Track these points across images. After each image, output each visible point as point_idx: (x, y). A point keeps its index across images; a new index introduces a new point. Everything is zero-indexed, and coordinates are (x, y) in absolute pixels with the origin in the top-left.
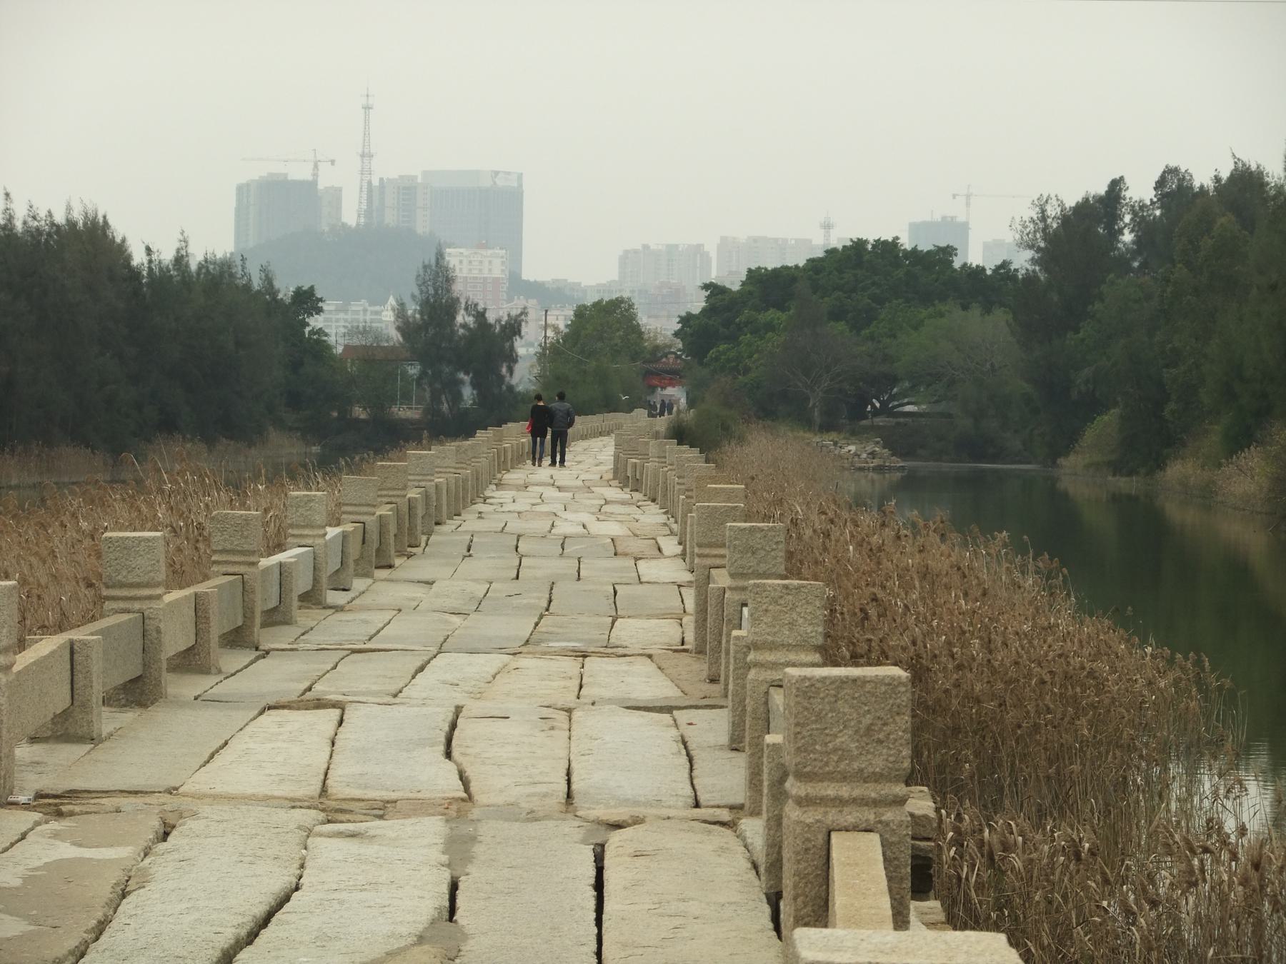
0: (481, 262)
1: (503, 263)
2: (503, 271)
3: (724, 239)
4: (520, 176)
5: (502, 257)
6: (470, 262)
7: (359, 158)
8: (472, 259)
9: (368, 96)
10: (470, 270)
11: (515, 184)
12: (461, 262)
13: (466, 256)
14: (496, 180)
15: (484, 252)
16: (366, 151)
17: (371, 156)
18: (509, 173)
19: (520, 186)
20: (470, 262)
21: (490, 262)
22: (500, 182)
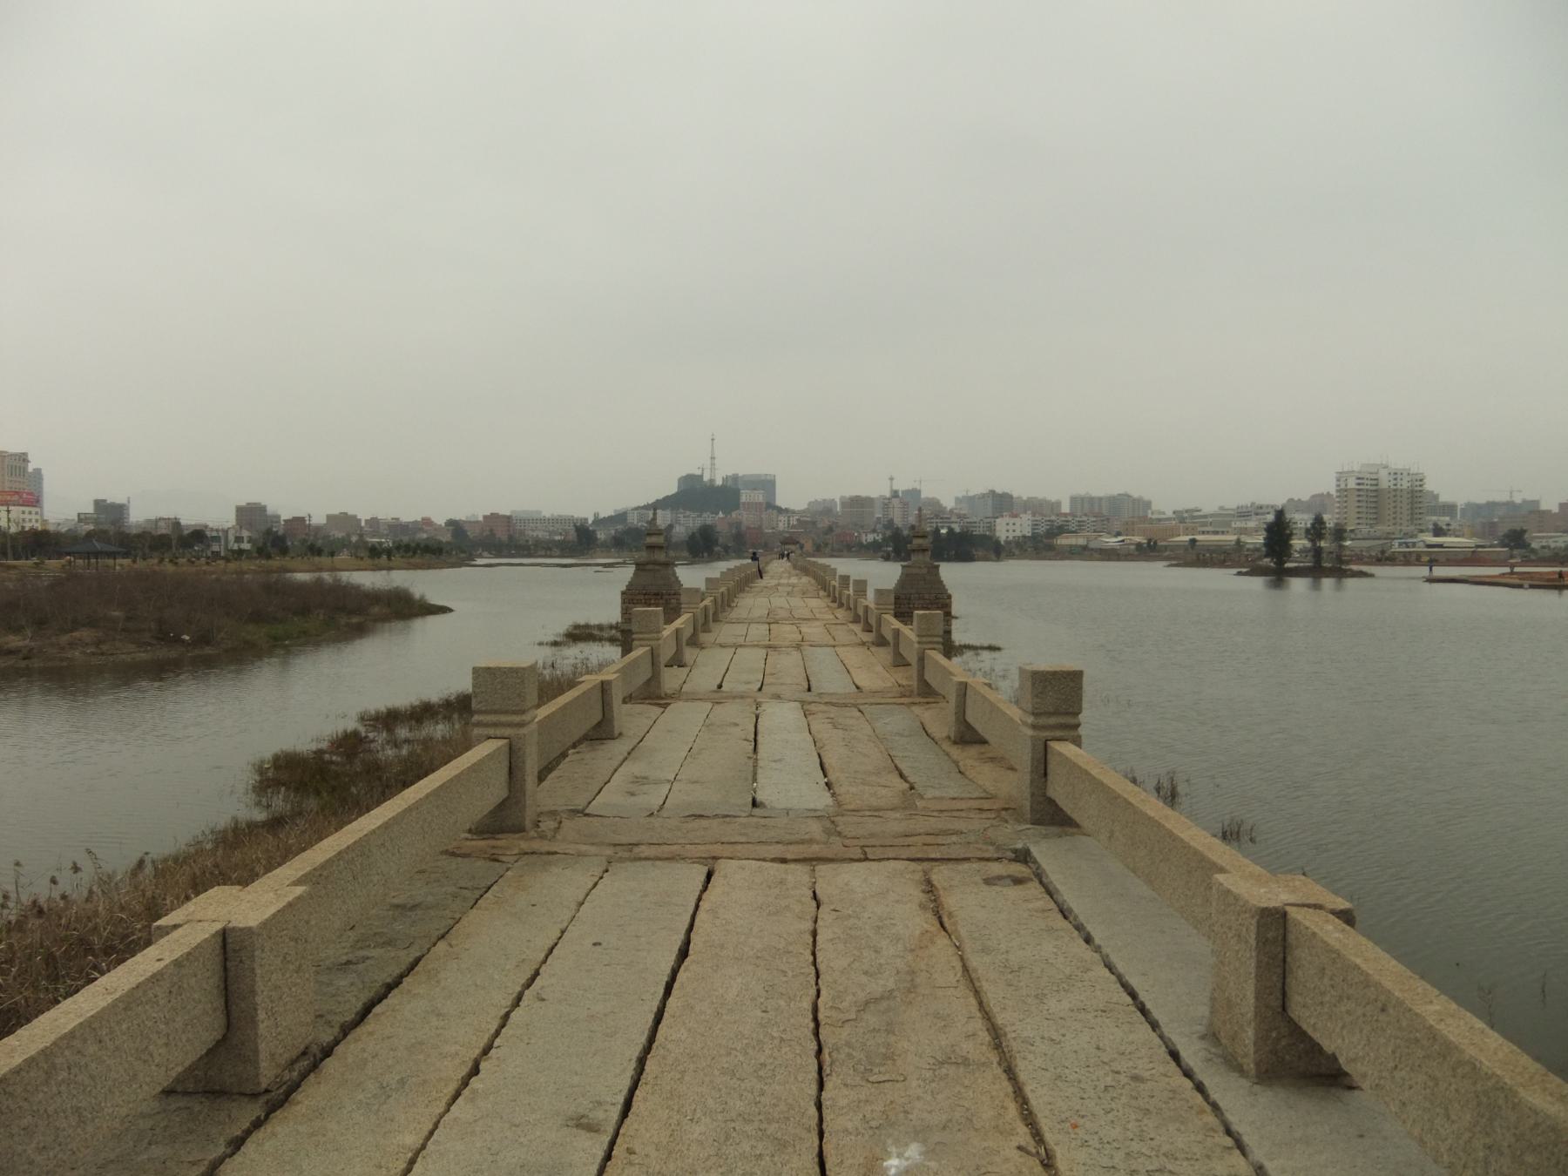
4: (775, 476)
15: (756, 492)
22: (768, 478)
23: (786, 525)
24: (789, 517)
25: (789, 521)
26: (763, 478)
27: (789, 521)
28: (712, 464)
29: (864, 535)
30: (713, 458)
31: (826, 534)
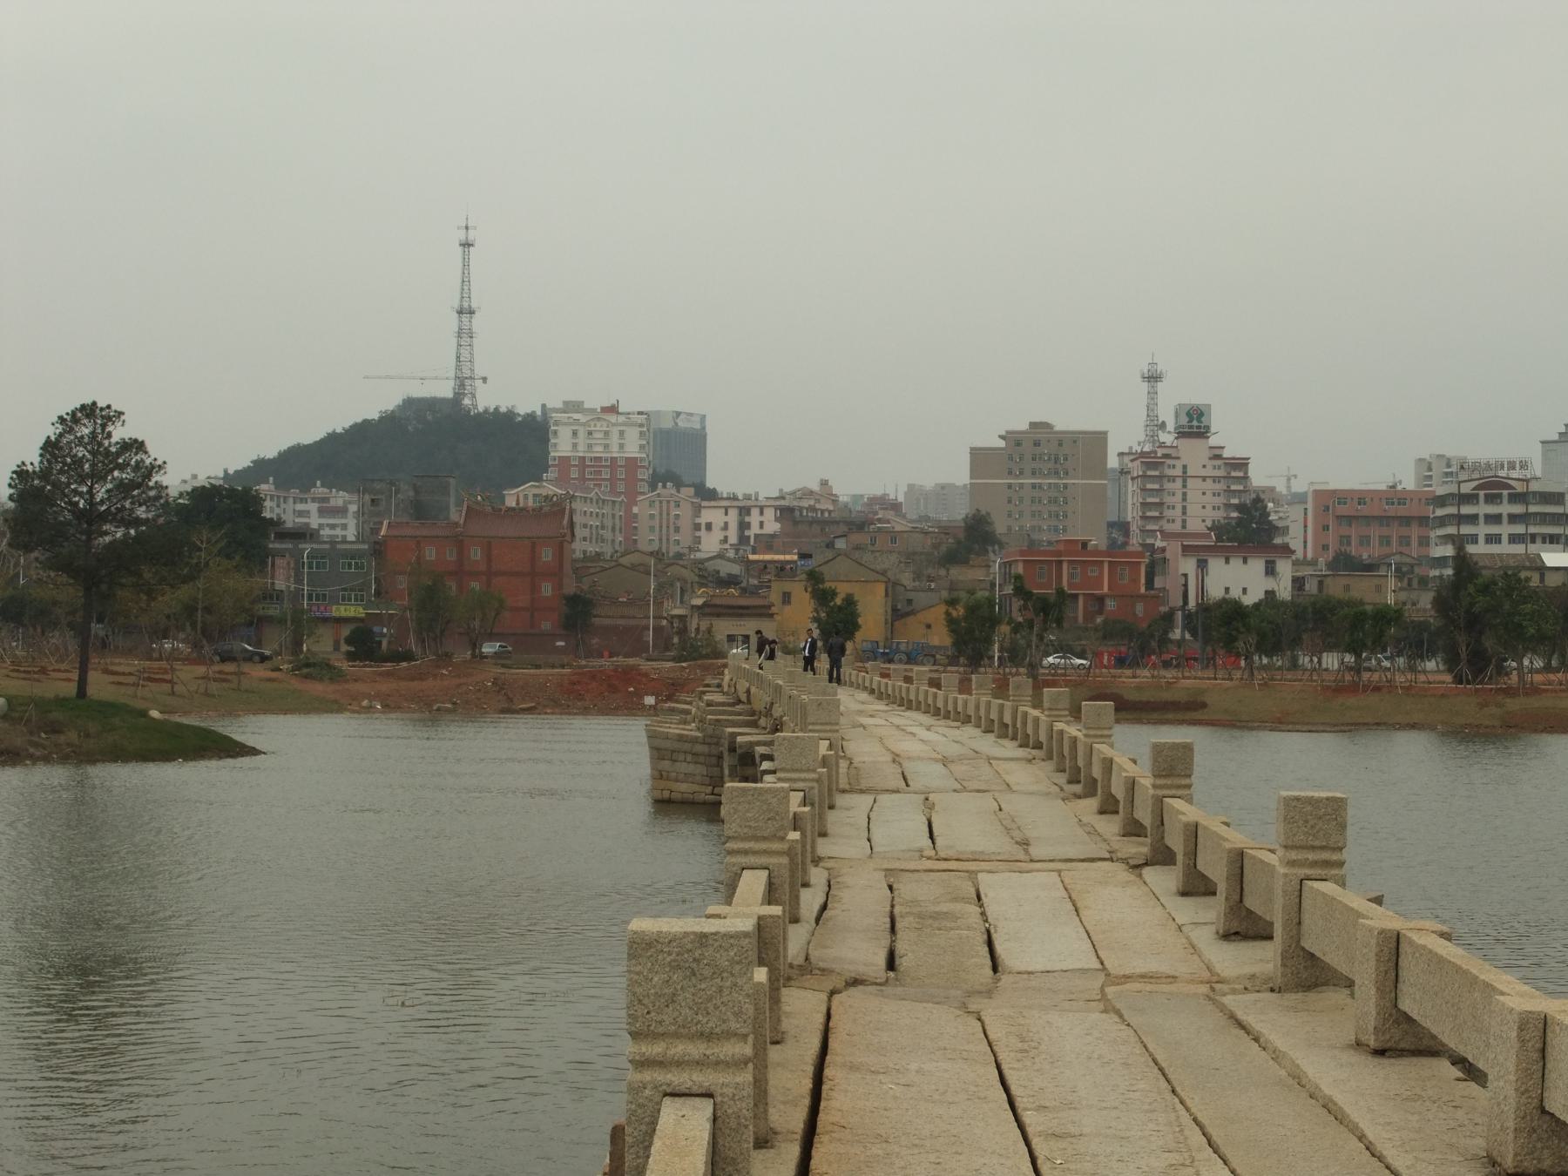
0: (606, 433)
1: (641, 433)
2: (642, 447)
3: (911, 487)
4: (703, 418)
5: (641, 425)
6: (590, 433)
7: (457, 315)
8: (593, 429)
9: (467, 228)
11: (698, 426)
12: (575, 433)
13: (584, 425)
14: (678, 421)
16: (466, 305)
17: (472, 312)
18: (691, 415)
19: (704, 428)
20: (590, 433)
21: (622, 433)
22: (682, 424)
23: (733, 539)
24: (744, 511)
25: (743, 526)
26: (667, 424)
27: (743, 526)
28: (459, 334)
29: (1188, 566)
30: (465, 311)
31: (954, 558)
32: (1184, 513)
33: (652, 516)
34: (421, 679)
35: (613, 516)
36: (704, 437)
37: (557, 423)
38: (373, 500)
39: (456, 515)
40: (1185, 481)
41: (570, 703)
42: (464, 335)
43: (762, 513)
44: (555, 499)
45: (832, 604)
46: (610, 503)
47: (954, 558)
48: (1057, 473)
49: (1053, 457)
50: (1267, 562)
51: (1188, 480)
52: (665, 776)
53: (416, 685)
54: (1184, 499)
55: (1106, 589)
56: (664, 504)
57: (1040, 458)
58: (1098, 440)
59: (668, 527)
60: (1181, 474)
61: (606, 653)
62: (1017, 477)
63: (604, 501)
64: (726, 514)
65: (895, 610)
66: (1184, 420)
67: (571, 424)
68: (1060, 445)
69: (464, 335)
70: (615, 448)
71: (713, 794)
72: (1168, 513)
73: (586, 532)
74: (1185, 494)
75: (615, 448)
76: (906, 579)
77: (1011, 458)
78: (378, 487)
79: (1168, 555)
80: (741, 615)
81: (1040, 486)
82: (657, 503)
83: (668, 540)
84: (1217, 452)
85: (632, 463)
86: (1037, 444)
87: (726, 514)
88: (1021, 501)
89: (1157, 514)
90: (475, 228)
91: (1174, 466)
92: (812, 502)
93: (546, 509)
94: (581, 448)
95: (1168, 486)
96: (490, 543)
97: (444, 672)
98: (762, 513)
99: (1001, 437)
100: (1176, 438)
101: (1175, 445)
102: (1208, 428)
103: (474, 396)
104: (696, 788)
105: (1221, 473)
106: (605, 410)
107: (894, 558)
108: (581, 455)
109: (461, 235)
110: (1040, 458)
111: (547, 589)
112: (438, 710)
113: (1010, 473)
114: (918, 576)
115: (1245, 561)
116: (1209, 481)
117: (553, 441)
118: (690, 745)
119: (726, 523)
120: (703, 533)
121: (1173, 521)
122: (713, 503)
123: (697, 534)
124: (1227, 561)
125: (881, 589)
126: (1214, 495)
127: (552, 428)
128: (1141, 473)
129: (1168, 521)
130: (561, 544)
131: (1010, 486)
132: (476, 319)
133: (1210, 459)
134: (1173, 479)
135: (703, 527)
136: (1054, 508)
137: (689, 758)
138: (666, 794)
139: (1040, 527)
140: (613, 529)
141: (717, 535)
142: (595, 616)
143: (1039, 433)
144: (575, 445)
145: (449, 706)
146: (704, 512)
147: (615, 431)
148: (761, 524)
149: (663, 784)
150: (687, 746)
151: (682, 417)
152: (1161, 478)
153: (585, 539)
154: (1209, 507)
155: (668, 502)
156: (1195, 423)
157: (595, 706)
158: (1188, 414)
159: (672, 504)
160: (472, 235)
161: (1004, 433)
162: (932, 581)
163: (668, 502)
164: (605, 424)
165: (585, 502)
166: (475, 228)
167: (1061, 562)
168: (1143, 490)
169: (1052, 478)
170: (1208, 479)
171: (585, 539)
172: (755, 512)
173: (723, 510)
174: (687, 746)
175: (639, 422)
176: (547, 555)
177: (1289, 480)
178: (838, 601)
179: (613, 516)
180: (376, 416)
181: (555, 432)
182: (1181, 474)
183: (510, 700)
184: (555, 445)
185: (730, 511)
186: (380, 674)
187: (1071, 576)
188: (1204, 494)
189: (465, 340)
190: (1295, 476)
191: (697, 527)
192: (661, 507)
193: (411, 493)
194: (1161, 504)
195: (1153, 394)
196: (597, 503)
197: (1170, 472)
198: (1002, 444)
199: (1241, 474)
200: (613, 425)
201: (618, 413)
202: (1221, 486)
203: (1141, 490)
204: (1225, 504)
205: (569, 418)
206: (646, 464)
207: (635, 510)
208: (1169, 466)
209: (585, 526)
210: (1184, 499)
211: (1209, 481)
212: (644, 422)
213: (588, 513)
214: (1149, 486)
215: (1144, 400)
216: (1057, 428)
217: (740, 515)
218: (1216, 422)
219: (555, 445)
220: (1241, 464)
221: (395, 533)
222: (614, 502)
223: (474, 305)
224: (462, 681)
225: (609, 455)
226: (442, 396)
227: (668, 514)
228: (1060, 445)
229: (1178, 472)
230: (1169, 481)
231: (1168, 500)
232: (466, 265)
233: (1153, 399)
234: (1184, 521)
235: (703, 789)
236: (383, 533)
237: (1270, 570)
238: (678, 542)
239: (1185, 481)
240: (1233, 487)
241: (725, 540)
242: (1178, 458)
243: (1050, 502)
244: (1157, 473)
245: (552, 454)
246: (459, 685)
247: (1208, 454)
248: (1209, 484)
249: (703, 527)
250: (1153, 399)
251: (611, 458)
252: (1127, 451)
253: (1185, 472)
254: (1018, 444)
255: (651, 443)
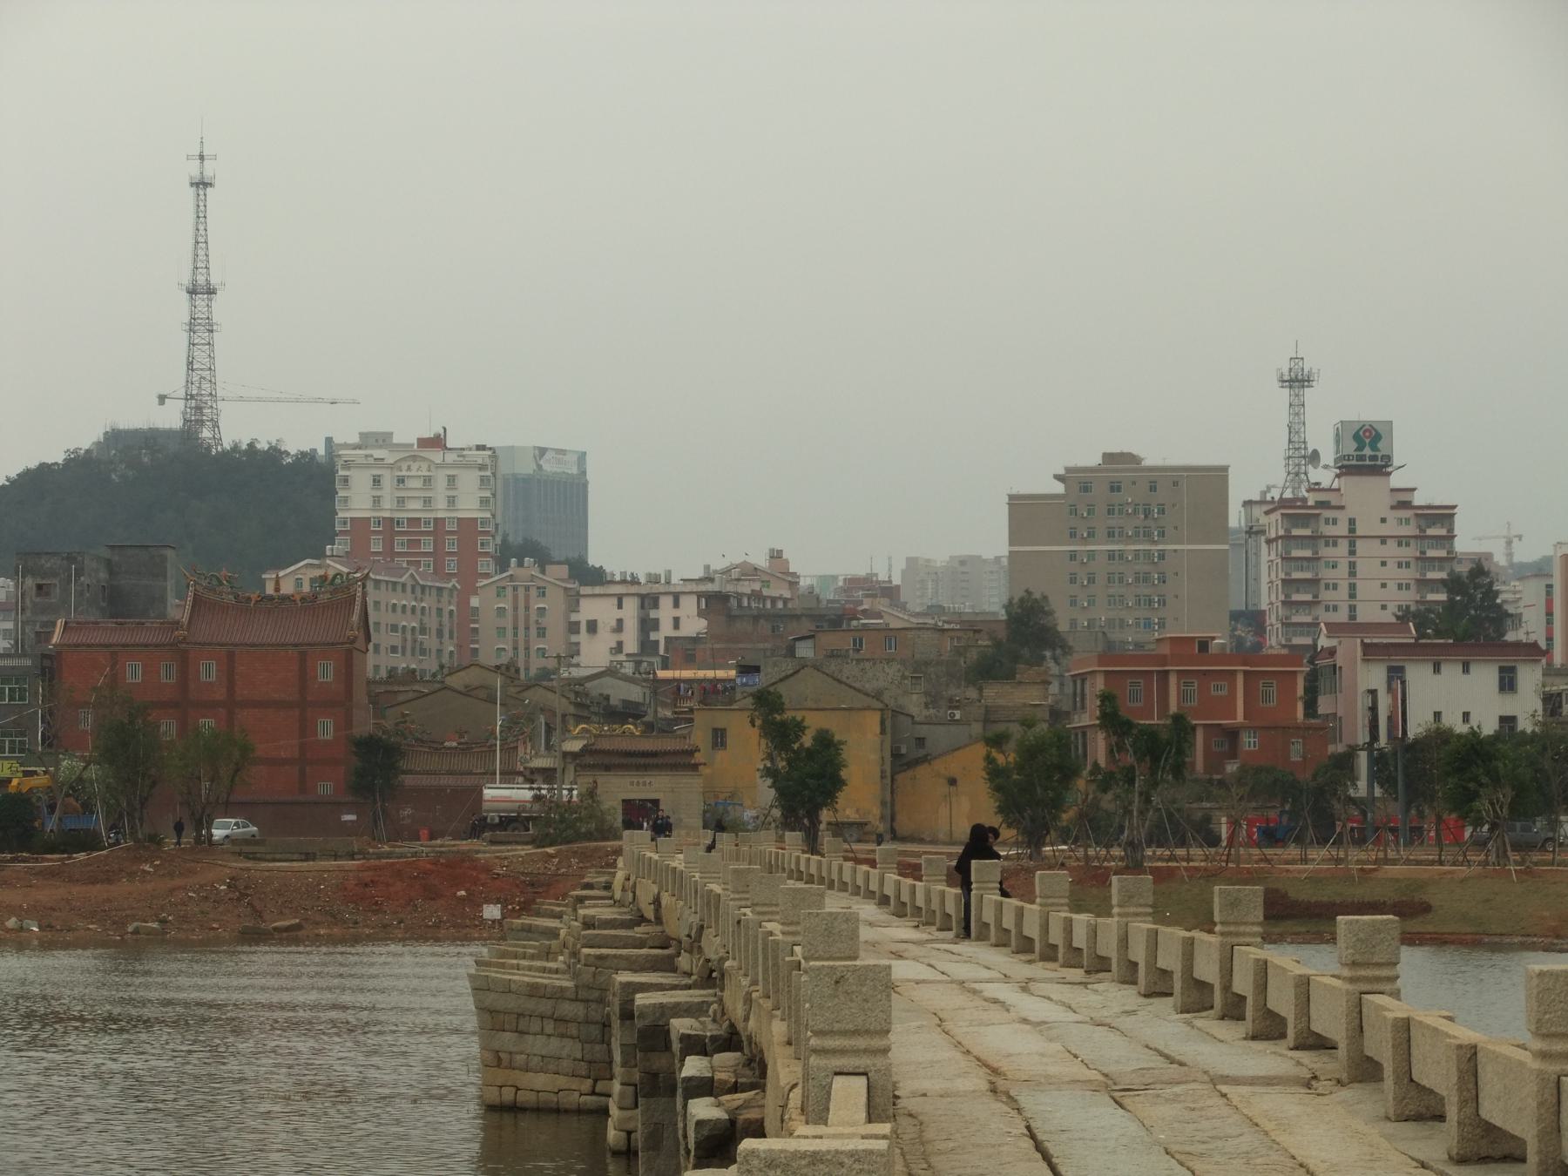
1: (482, 479)
3: (911, 562)
4: (582, 457)
5: (482, 467)
6: (401, 480)
9: (202, 157)
10: (401, 501)
11: (574, 471)
12: (377, 481)
13: (391, 467)
14: (541, 462)
16: (201, 280)
17: (211, 291)
18: (562, 452)
19: (584, 473)
20: (401, 480)
21: (452, 480)
22: (549, 467)
23: (631, 646)
24: (649, 601)
25: (648, 625)
26: (526, 467)
27: (648, 625)
28: (191, 330)
29: (1374, 676)
30: (201, 290)
31: (991, 669)
32: (1352, 596)
33: (501, 611)
34: (109, 881)
35: (440, 610)
36: (585, 485)
37: (347, 465)
38: (39, 587)
39: (177, 609)
40: (1352, 544)
41: (359, 918)
42: (199, 327)
43: (676, 605)
44: (338, 581)
45: (796, 746)
46: (434, 592)
47: (991, 669)
48: (1148, 535)
49: (1141, 508)
50: (1502, 670)
51: (1359, 543)
52: (505, 1063)
53: (98, 891)
54: (1352, 573)
55: (1240, 718)
56: (521, 591)
57: (1120, 512)
58: (1214, 479)
59: (527, 628)
60: (1345, 533)
61: (424, 833)
62: (1084, 541)
63: (423, 588)
64: (620, 606)
65: (896, 755)
66: (1350, 447)
67: (367, 466)
68: (1153, 488)
69: (199, 327)
70: (441, 503)
71: (593, 1093)
72: (1326, 596)
73: (395, 639)
74: (1352, 565)
75: (441, 503)
76: (914, 704)
77: (1074, 511)
78: (48, 565)
79: (1340, 660)
80: (646, 767)
81: (1121, 554)
82: (509, 591)
83: (527, 649)
84: (1403, 497)
85: (467, 525)
86: (1115, 488)
87: (620, 606)
88: (1091, 580)
89: (1308, 597)
90: (215, 157)
91: (1335, 522)
92: (757, 586)
93: (324, 598)
94: (387, 504)
95: (1326, 552)
96: (231, 655)
97: (147, 868)
98: (676, 605)
99: (1058, 478)
100: (1338, 476)
101: (1335, 485)
102: (1388, 459)
103: (216, 425)
104: (562, 1082)
105: (1410, 530)
106: (424, 443)
107: (893, 671)
108: (387, 515)
109: (193, 169)
110: (1120, 512)
111: (326, 730)
112: (136, 932)
113: (1073, 535)
114: (932, 700)
115: (1466, 670)
116: (1392, 543)
117: (341, 494)
118: (550, 1003)
119: (620, 621)
120: (583, 637)
121: (1335, 608)
122: (598, 590)
123: (574, 638)
124: (1437, 669)
125: (873, 720)
126: (1400, 565)
127: (341, 473)
128: (1281, 532)
129: (1327, 609)
130: (349, 652)
131: (1073, 556)
132: (219, 300)
133: (1393, 508)
134: (1333, 541)
135: (583, 627)
136: (1144, 590)
137: (549, 1027)
138: (508, 1095)
139: (1122, 620)
140: (440, 633)
141: (605, 640)
142: (404, 772)
143: (1117, 471)
144: (377, 500)
145: (155, 925)
146: (584, 603)
147: (440, 479)
148: (676, 623)
149: (501, 1075)
150: (545, 1006)
151: (548, 455)
152: (1314, 539)
153: (394, 649)
154: (1392, 585)
155: (527, 589)
156: (1367, 452)
157: (400, 923)
158: (1356, 437)
159: (533, 592)
160: (210, 169)
161: (1062, 472)
162: (957, 708)
163: (527, 589)
164: (424, 466)
165: (394, 590)
166: (215, 157)
167: (1167, 672)
168: (1286, 559)
169: (1140, 543)
170: (1389, 541)
171: (394, 649)
172: (666, 602)
173: (615, 601)
174: (545, 1006)
175: (480, 461)
176: (325, 673)
177: (1509, 543)
178: (807, 740)
179: (440, 610)
180: (59, 458)
181: (346, 480)
182: (1345, 533)
183: (258, 914)
184: (346, 499)
185: (625, 601)
186: (41, 873)
187: (1182, 696)
188: (1384, 564)
189: (201, 336)
190: (1520, 537)
191: (574, 628)
192: (516, 598)
193: (103, 575)
194: (1314, 582)
195: (1297, 408)
196: (413, 592)
197: (1329, 530)
198: (1059, 488)
199: (1443, 532)
200: (438, 466)
201: (445, 447)
202: (1410, 552)
203: (1283, 559)
204: (1418, 581)
205: (366, 456)
206: (491, 529)
207: (475, 602)
208: (1327, 521)
209: (394, 628)
210: (1352, 573)
211: (1392, 543)
212: (488, 461)
213: (399, 609)
214: (1296, 553)
215: (1284, 417)
216: (1147, 463)
217: (642, 606)
218: (1401, 449)
219: (346, 499)
220: (1443, 516)
221: (74, 638)
222: (440, 589)
223: (214, 281)
224: (178, 882)
225: (433, 515)
226: (167, 426)
227: (527, 608)
228: (1153, 488)
229: (1342, 529)
230: (1327, 545)
231: (1327, 574)
232: (200, 216)
233: (1297, 414)
234: (1352, 609)
235: (575, 1084)
236: (55, 639)
237: (1507, 683)
238: (542, 652)
239: (1352, 544)
240: (1431, 553)
241: (619, 648)
242: (1342, 508)
243: (1137, 580)
244: (1307, 532)
245: (341, 515)
246: (172, 891)
247: (1388, 500)
248: (1392, 549)
249: (583, 627)
250: (1297, 414)
251: (436, 520)
252: (1257, 498)
253: (1352, 530)
254: (1086, 488)
255: (500, 496)
